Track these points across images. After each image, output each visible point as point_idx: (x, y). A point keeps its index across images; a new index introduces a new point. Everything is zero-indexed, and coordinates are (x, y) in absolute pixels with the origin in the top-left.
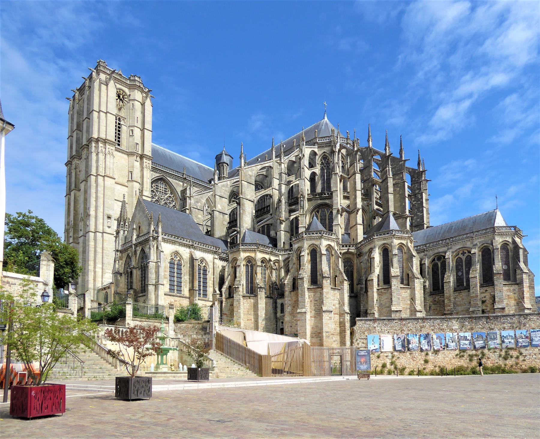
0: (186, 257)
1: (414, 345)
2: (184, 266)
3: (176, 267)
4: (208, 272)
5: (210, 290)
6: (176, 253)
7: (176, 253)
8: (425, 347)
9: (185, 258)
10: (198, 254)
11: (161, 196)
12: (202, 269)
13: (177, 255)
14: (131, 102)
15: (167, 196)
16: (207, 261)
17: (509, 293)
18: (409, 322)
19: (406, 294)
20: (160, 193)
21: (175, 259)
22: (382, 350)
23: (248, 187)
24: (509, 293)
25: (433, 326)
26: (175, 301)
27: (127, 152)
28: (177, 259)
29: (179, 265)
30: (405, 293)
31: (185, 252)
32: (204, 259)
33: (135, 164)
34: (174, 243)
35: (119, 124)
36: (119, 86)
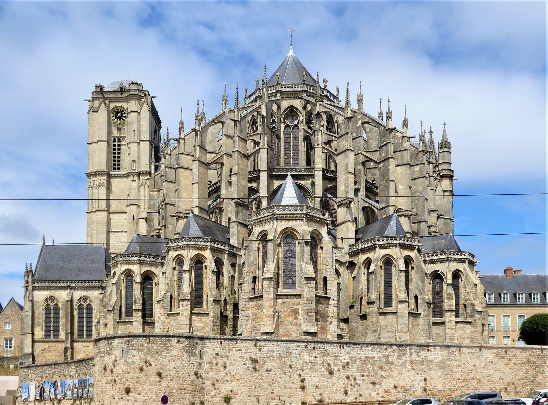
1: (46, 394)
3: (52, 311)
6: (52, 298)
7: (52, 298)
8: (53, 396)
9: (63, 300)
10: (78, 294)
12: (85, 308)
13: (54, 300)
14: (129, 116)
16: (92, 298)
17: (256, 311)
18: (47, 369)
19: (176, 321)
21: (51, 304)
22: (29, 400)
24: (256, 311)
27: (124, 174)
28: (54, 304)
29: (57, 309)
30: (174, 320)
31: (62, 295)
32: (88, 297)
33: (132, 185)
34: (48, 288)
35: (119, 145)
36: (112, 105)
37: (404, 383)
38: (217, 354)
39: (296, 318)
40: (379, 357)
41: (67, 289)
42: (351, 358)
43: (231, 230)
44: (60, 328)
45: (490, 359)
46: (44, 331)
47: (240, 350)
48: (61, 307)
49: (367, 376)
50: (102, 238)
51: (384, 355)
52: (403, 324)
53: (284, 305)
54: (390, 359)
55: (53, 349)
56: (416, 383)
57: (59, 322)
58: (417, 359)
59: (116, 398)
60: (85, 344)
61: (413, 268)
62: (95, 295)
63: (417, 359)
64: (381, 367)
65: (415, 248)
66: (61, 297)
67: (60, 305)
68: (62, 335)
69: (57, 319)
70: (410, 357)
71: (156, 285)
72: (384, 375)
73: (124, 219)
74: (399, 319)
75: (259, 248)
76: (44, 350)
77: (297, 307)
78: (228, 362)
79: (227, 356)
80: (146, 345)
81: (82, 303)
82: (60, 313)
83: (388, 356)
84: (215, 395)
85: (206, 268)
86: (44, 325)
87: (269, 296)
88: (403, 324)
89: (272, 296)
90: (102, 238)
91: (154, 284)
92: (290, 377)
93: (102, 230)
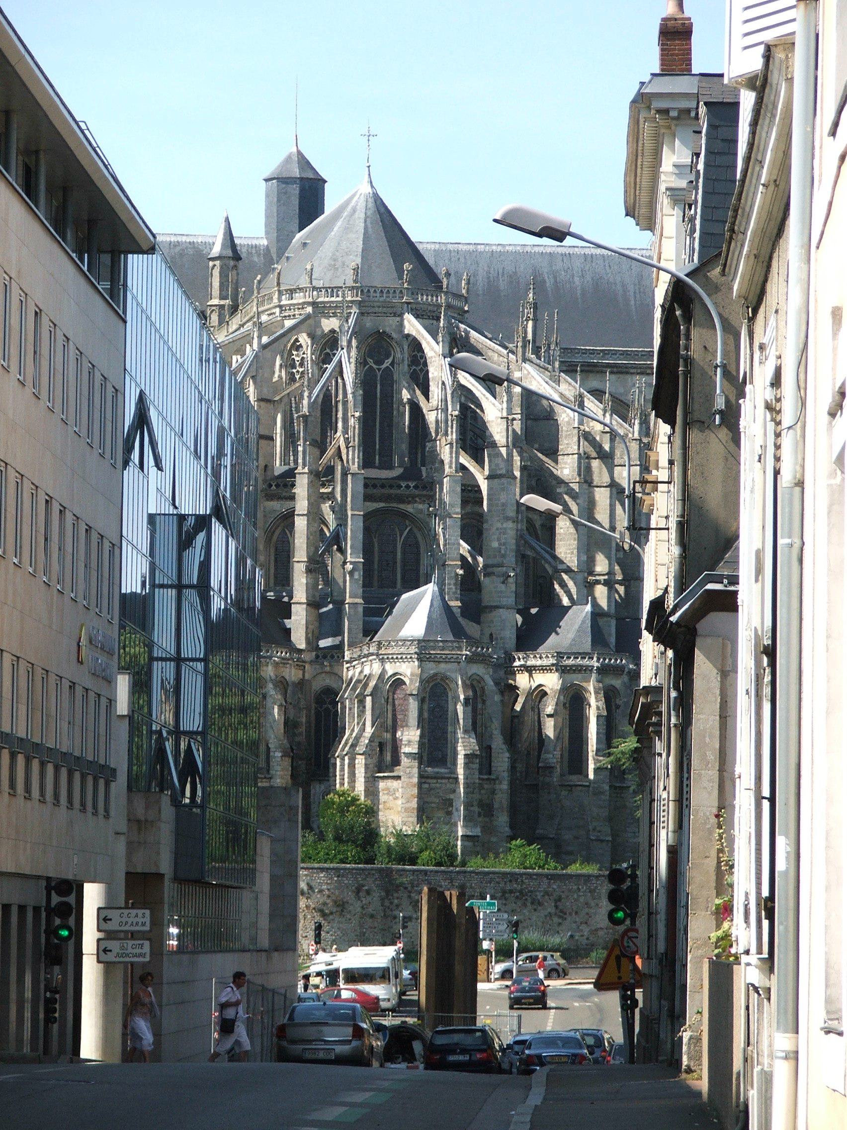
53: (432, 792)
61: (618, 707)
75: (388, 698)
77: (452, 796)
80: (336, 879)
87: (411, 780)
89: (415, 780)
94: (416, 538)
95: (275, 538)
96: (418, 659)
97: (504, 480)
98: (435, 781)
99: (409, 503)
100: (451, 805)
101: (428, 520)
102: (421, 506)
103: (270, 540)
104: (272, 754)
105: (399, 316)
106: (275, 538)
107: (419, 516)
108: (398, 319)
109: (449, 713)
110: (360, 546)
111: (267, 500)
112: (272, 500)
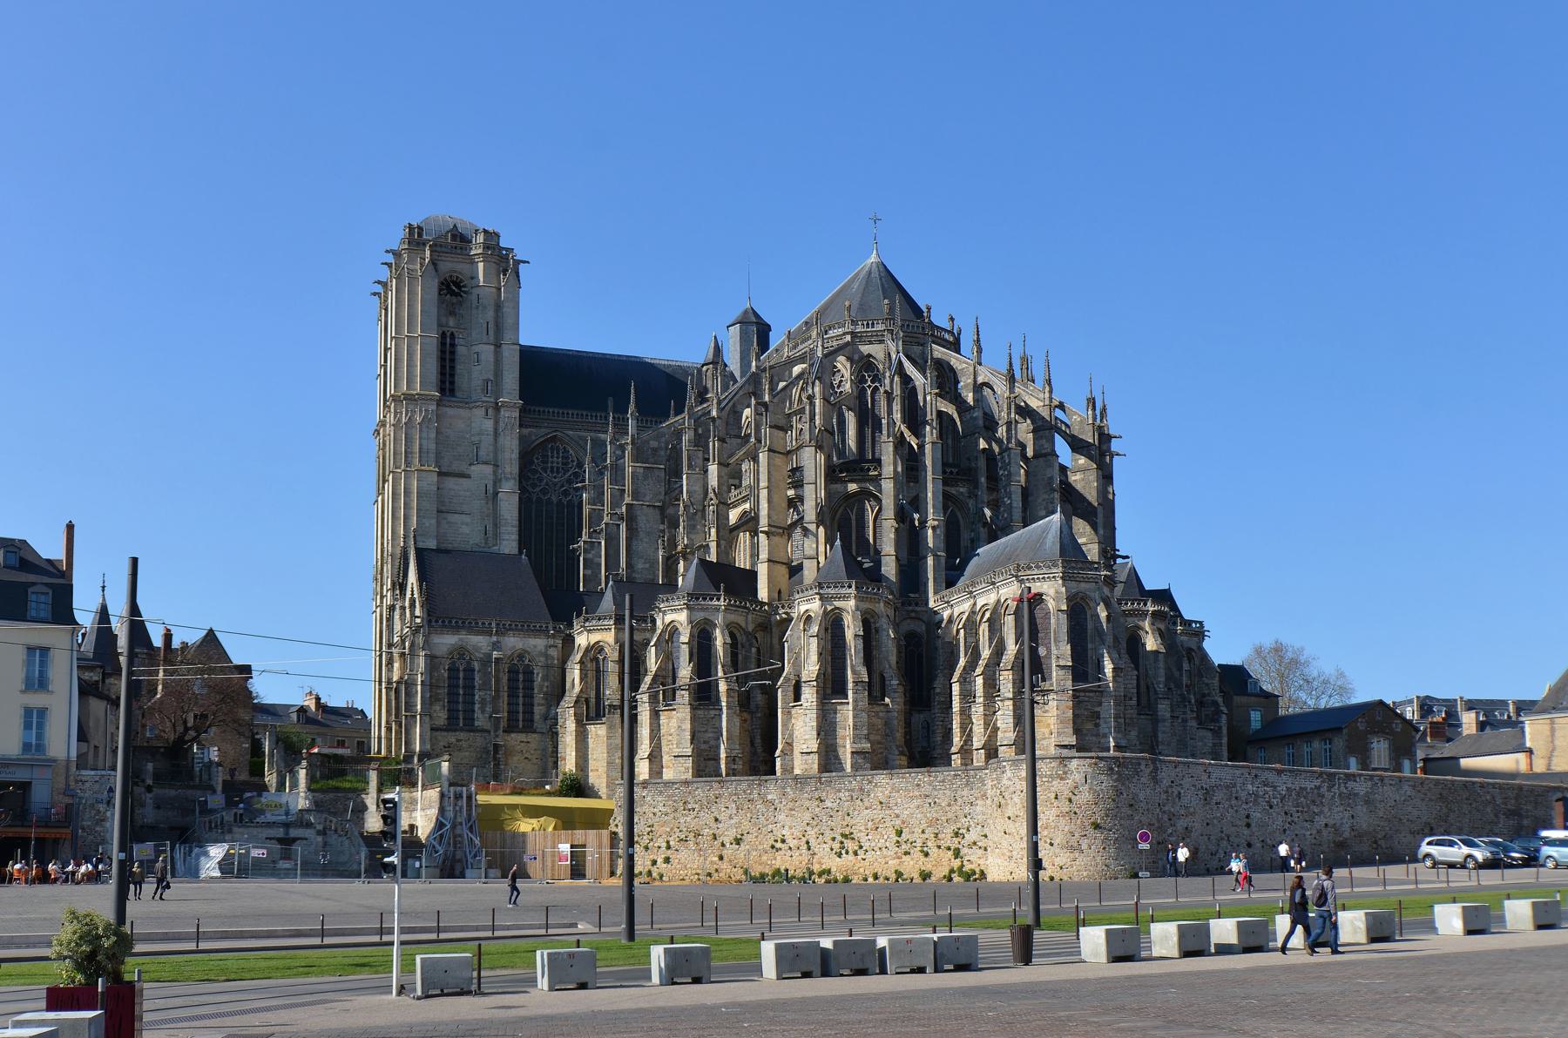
0: (483, 654)
2: (479, 671)
4: (535, 675)
5: (538, 711)
7: (461, 652)
9: (482, 656)
11: (555, 478)
15: (570, 473)
20: (552, 471)
23: (646, 477)
25: (735, 794)
26: (458, 740)
29: (470, 671)
31: (479, 642)
32: (527, 651)
34: (456, 629)
37: (1333, 822)
38: (1172, 782)
39: (1097, 725)
40: (1311, 788)
41: (491, 635)
42: (1288, 789)
43: (882, 569)
44: (477, 706)
45: (1409, 793)
46: (446, 712)
47: (1192, 777)
48: (477, 668)
49: (1302, 811)
50: (427, 525)
51: (1316, 786)
52: (1164, 732)
54: (1322, 790)
55: (464, 744)
56: (1344, 821)
57: (474, 695)
58: (1345, 791)
59: (1077, 835)
60: (522, 737)
62: (539, 648)
63: (1345, 791)
64: (1313, 801)
65: (1166, 618)
66: (477, 649)
67: (476, 665)
68: (481, 720)
69: (470, 687)
70: (1339, 789)
71: (743, 647)
72: (1316, 811)
73: (465, 491)
74: (1160, 725)
76: (449, 747)
77: (1098, 709)
78: (1182, 791)
79: (1181, 785)
81: (516, 662)
82: (477, 679)
83: (1318, 788)
84: (1171, 833)
85: (877, 631)
86: (446, 700)
88: (1164, 732)
90: (427, 525)
91: (739, 646)
92: (1237, 811)
93: (427, 510)
94: (956, 516)
95: (837, 518)
96: (1062, 578)
97: (1049, 457)
98: (1083, 694)
99: (953, 486)
100: (1099, 718)
101: (967, 501)
102: (961, 490)
103: (834, 519)
104: (887, 683)
105: (922, 345)
106: (837, 518)
107: (961, 497)
108: (921, 348)
109: (1089, 631)
110: (940, 506)
111: (832, 483)
112: (836, 483)
